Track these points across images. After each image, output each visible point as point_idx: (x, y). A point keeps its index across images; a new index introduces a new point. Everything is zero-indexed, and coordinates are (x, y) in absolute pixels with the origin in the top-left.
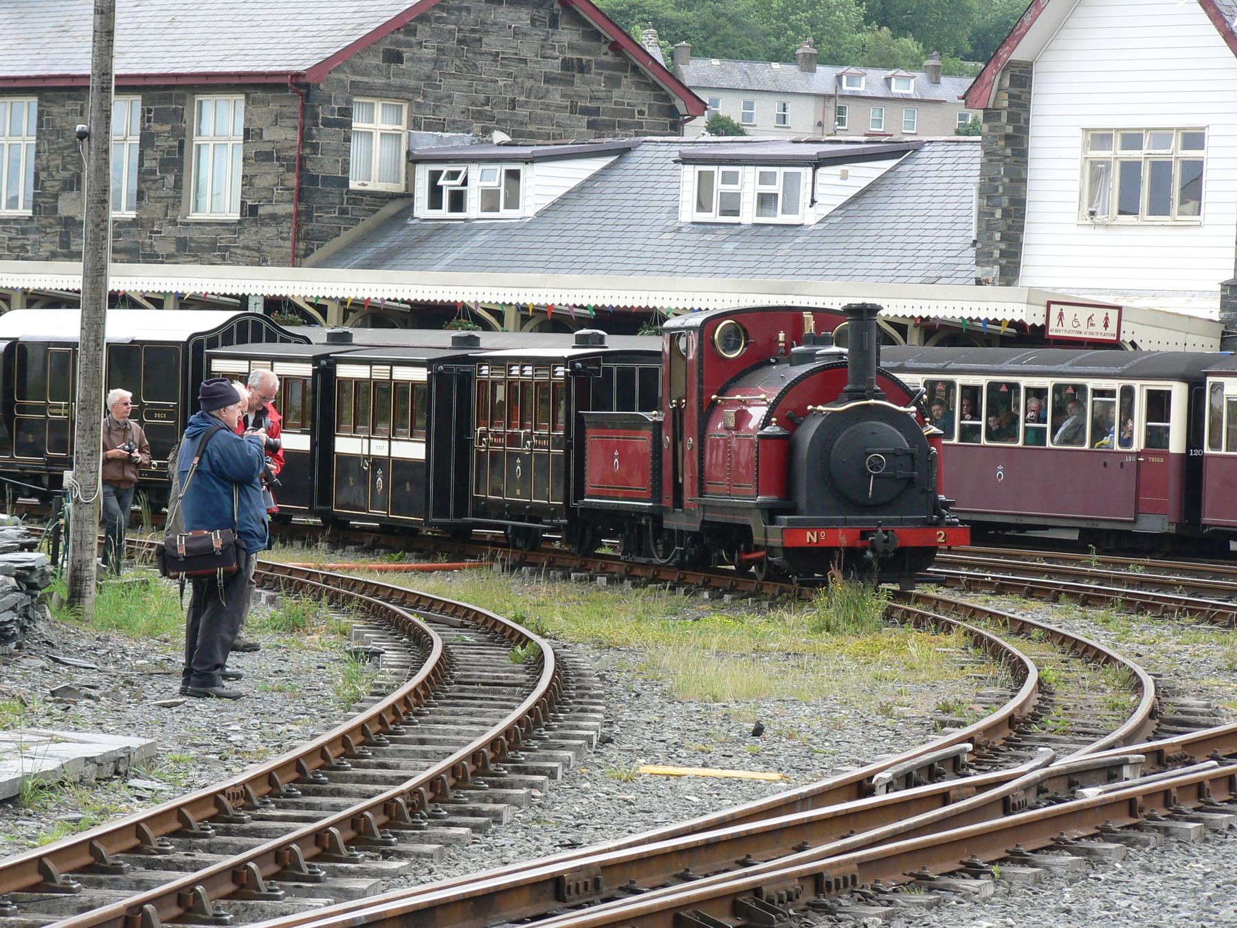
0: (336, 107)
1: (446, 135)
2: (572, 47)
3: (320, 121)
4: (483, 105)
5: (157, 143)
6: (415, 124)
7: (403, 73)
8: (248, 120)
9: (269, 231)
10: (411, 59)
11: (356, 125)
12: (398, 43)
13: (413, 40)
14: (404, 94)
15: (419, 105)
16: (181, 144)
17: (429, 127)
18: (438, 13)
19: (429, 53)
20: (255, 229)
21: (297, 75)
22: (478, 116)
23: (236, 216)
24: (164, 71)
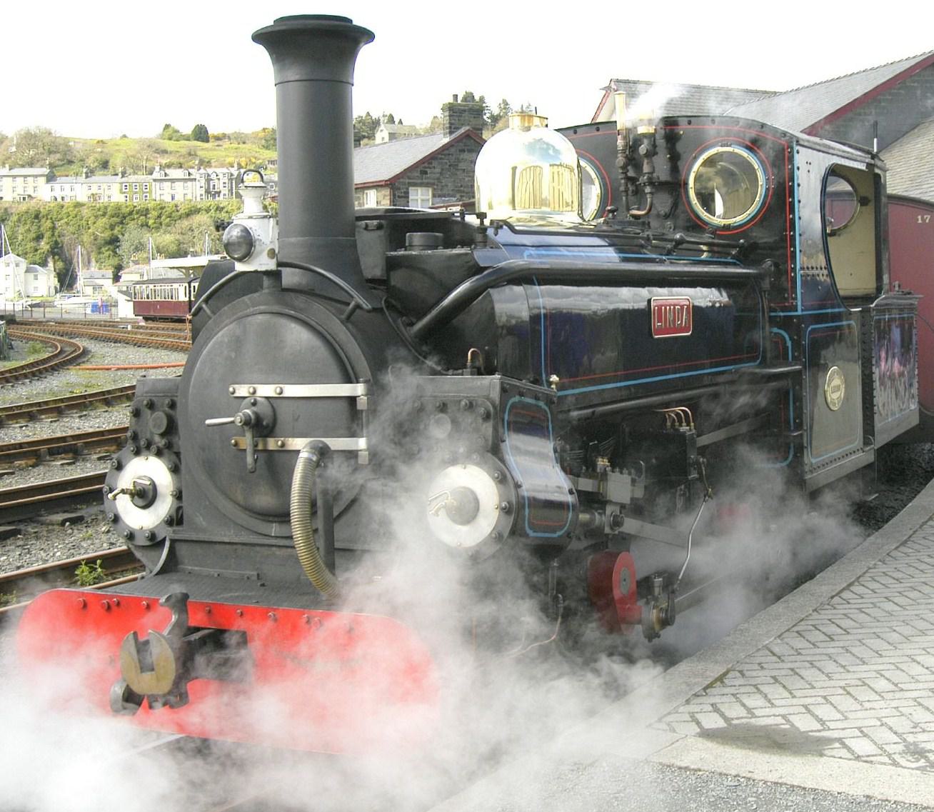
1: (447, 199)
6: (434, 196)
7: (428, 178)
10: (430, 173)
11: (411, 197)
12: (425, 167)
13: (431, 166)
15: (435, 189)
17: (440, 196)
18: (440, 156)
19: (438, 170)
22: (459, 191)
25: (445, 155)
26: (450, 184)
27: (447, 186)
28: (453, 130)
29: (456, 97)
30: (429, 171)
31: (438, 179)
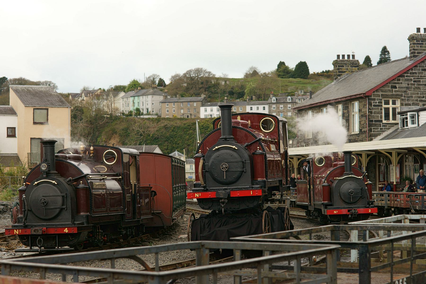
0: (377, 101)
3: (373, 106)
4: (422, 98)
5: (345, 115)
6: (402, 104)
8: (359, 107)
9: (364, 136)
10: (399, 87)
14: (398, 97)
15: (402, 100)
16: (349, 114)
17: (406, 105)
20: (361, 135)
21: (364, 94)
22: (421, 101)
23: (358, 133)
24: (343, 97)
25: (410, 73)
29: (418, 30)
30: (397, 86)
31: (405, 92)
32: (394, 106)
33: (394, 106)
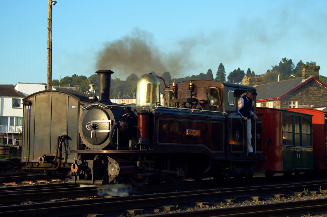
2: (324, 92)
6: (298, 104)
7: (296, 97)
17: (300, 105)
18: (301, 88)
22: (309, 103)
26: (305, 100)
27: (304, 100)
28: (306, 77)
31: (300, 97)
32: (294, 105)
33: (294, 105)
